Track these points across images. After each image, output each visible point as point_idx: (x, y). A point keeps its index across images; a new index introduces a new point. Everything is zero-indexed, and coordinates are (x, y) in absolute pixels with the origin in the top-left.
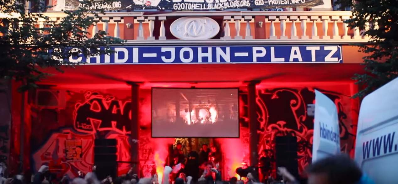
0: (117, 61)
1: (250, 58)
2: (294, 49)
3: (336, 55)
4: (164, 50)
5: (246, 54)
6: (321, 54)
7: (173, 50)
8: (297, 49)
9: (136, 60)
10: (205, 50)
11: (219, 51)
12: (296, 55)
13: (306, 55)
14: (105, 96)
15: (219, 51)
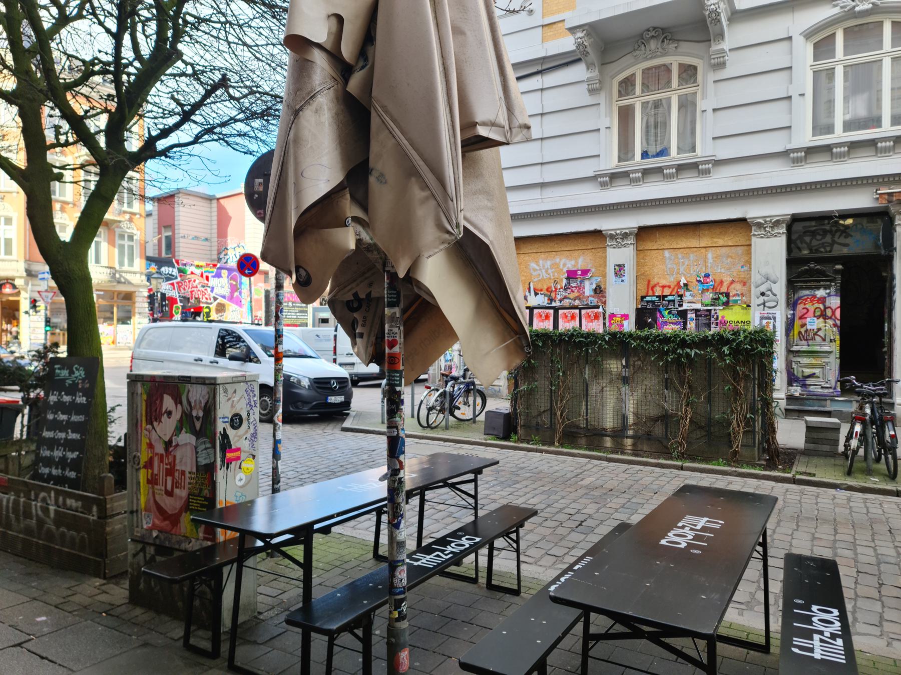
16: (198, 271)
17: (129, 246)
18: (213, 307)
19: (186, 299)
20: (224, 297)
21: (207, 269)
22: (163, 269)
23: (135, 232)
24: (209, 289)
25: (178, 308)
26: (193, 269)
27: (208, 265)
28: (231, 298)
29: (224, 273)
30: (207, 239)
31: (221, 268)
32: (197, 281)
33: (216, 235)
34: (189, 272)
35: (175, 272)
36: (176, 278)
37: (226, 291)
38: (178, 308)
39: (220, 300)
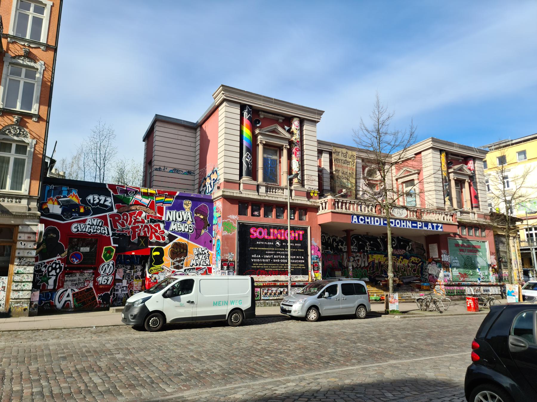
0: (376, 224)
1: (417, 227)
2: (430, 224)
3: (441, 228)
4: (391, 220)
5: (416, 225)
6: (437, 227)
7: (394, 221)
8: (430, 224)
9: (382, 224)
10: (403, 222)
11: (408, 222)
12: (430, 226)
13: (433, 227)
14: (326, 234)
15: (408, 222)
16: (146, 201)
17: (16, 161)
18: (167, 249)
19: (122, 239)
20: (185, 235)
21: (158, 199)
22: (90, 197)
23: (28, 140)
24: (162, 226)
25: (109, 251)
26: (138, 197)
27: (160, 194)
28: (196, 237)
29: (188, 205)
30: (189, 173)
31: (181, 198)
32: (144, 214)
33: (198, 167)
34: (132, 202)
35: (110, 201)
36: (111, 209)
37: (189, 227)
38: (109, 251)
39: (179, 239)
